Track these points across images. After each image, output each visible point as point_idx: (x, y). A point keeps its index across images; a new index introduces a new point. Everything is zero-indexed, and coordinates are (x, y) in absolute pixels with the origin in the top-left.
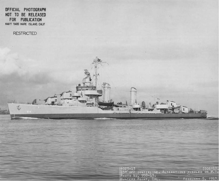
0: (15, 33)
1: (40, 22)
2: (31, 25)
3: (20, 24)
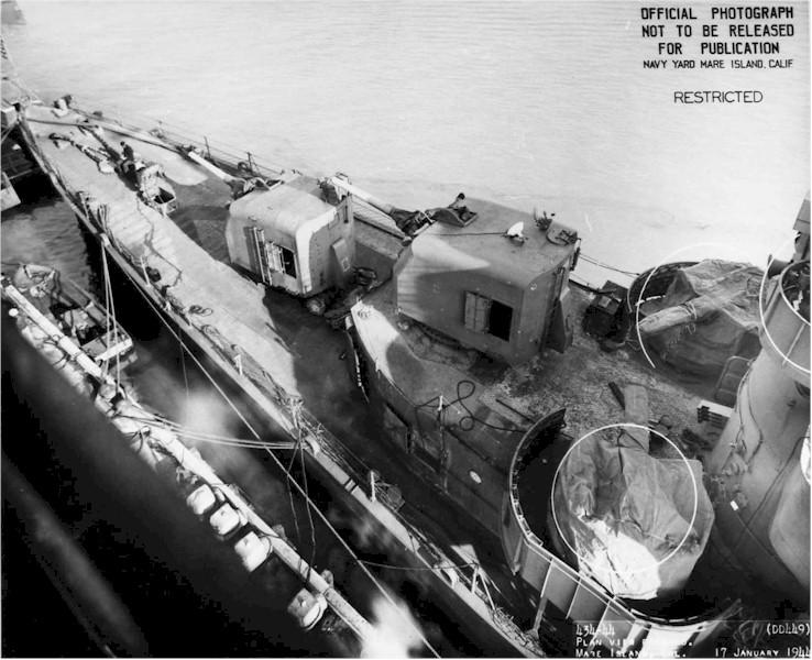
0: (683, 97)
2: (740, 66)
3: (698, 64)
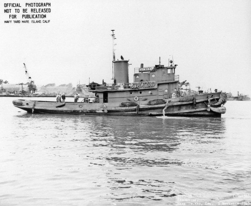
1: (45, 19)
3: (21, 22)
